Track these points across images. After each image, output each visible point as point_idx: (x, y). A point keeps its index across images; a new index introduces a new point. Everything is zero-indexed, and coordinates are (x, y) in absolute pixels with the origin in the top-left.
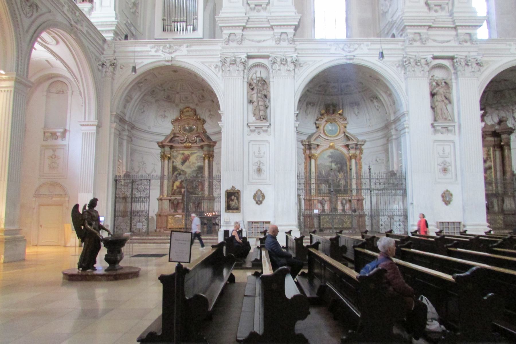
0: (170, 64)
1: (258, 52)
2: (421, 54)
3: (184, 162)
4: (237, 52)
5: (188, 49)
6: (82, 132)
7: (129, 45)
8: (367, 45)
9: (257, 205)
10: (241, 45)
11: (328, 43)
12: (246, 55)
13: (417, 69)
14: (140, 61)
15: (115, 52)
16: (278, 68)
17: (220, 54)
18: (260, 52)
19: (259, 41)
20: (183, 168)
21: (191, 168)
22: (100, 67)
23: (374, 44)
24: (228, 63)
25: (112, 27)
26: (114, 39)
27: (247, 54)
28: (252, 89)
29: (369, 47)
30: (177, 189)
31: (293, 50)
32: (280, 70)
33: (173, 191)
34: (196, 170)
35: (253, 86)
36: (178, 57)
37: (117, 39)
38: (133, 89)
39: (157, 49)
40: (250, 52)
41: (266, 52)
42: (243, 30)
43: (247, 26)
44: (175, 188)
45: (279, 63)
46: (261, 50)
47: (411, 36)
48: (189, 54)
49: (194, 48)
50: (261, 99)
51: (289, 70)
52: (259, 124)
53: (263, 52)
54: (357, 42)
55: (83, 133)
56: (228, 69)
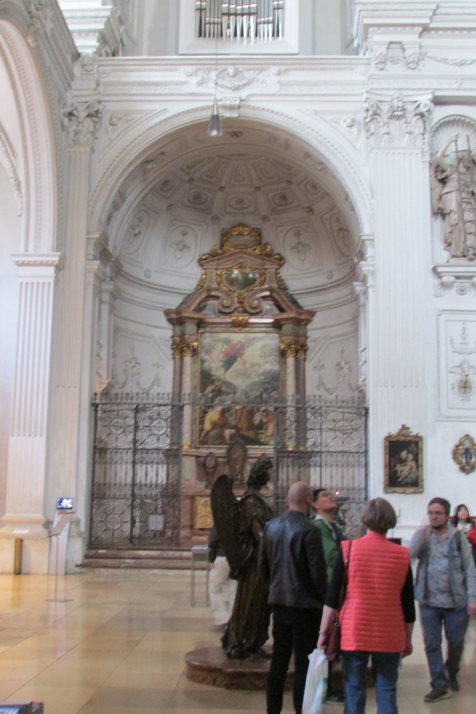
0: (235, 114)
1: (458, 89)
4: (407, 89)
6: (20, 280)
7: (133, 68)
9: (463, 475)
10: (416, 72)
12: (430, 96)
14: (159, 107)
15: (98, 85)
17: (367, 92)
18: (465, 90)
19: (462, 64)
21: (248, 377)
22: (66, 120)
24: (385, 116)
25: (96, 22)
26: (98, 53)
27: (433, 93)
28: (443, 181)
30: (212, 429)
34: (262, 383)
35: (445, 174)
36: (252, 99)
38: (132, 177)
40: (439, 90)
42: (420, 35)
43: (432, 25)
44: (207, 426)
48: (282, 92)
49: (294, 76)
50: (469, 206)
55: (21, 284)
56: (385, 130)
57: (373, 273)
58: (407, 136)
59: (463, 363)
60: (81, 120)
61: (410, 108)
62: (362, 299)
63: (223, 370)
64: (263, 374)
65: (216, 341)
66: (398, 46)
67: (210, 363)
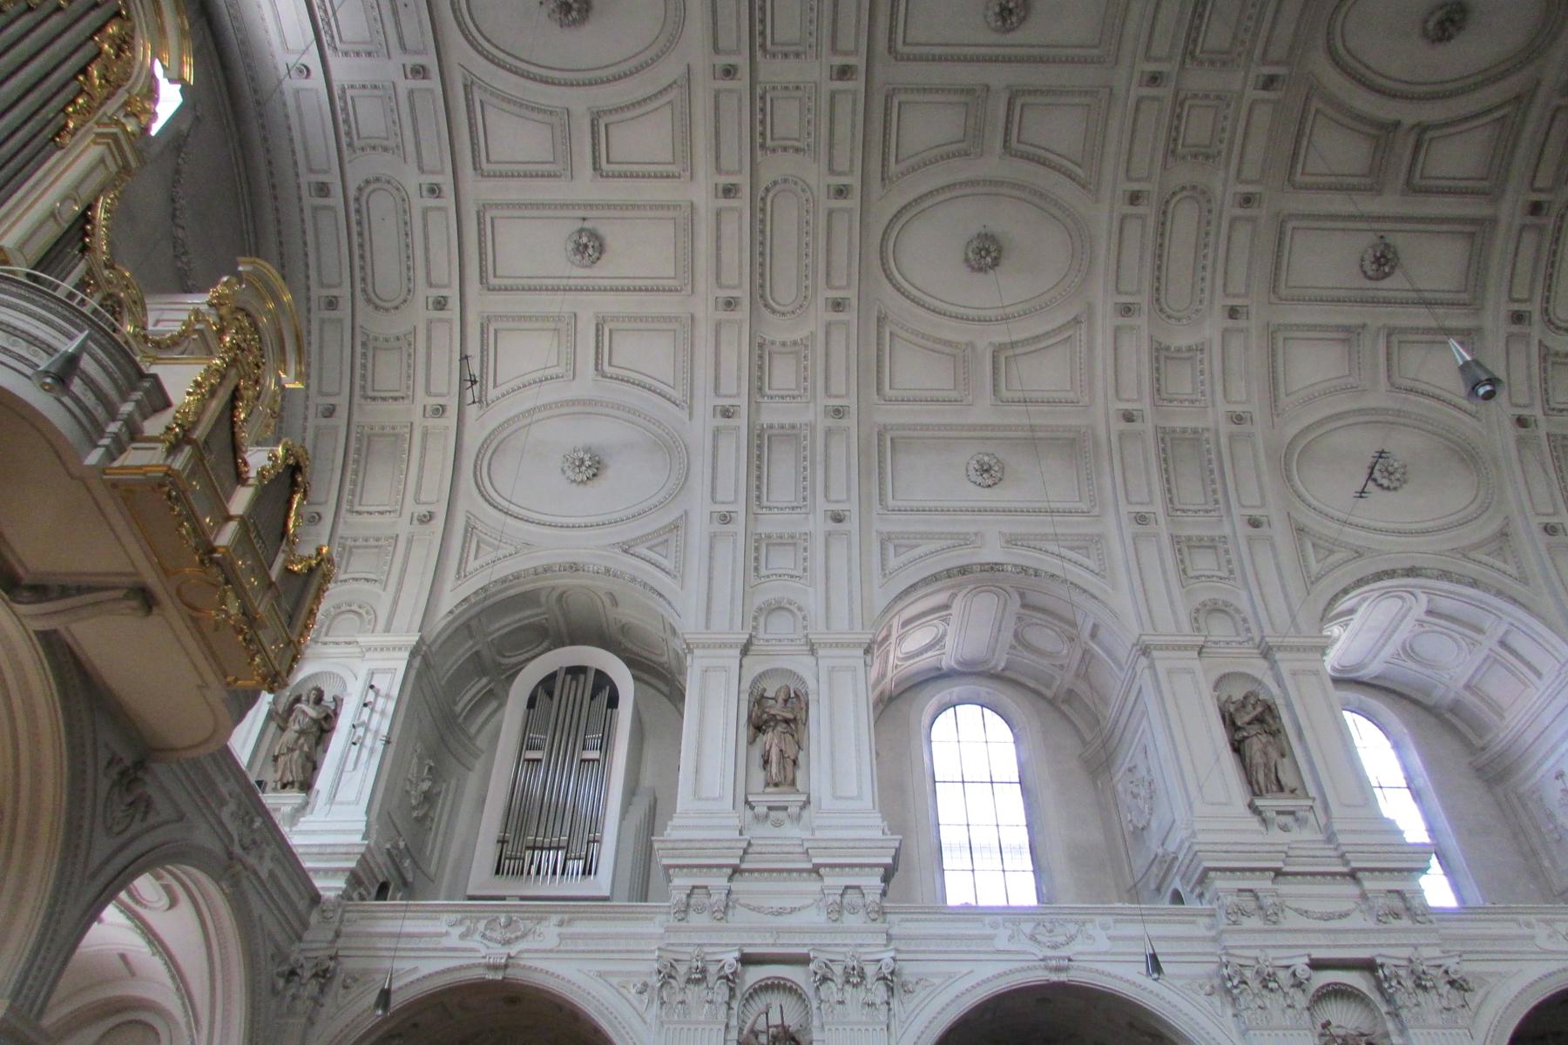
0: (499, 976)
1: (774, 945)
2: (1272, 953)
5: (564, 930)
7: (386, 915)
8: (1104, 927)
10: (723, 924)
11: (987, 919)
12: (737, 954)
13: (1268, 999)
14: (407, 965)
15: (338, 935)
16: (838, 997)
17: (659, 949)
18: (782, 945)
19: (780, 912)
22: (281, 983)
23: (1122, 921)
24: (681, 980)
25: (347, 860)
26: (346, 896)
29: (1111, 932)
31: (882, 939)
32: (841, 1002)
36: (526, 955)
37: (355, 895)
39: (468, 929)
40: (750, 945)
41: (797, 945)
42: (730, 879)
43: (744, 866)
45: (839, 981)
46: (785, 939)
47: (1230, 900)
48: (562, 948)
49: (581, 927)
51: (871, 1005)
54: (1074, 917)
56: (680, 997)
58: (707, 1005)
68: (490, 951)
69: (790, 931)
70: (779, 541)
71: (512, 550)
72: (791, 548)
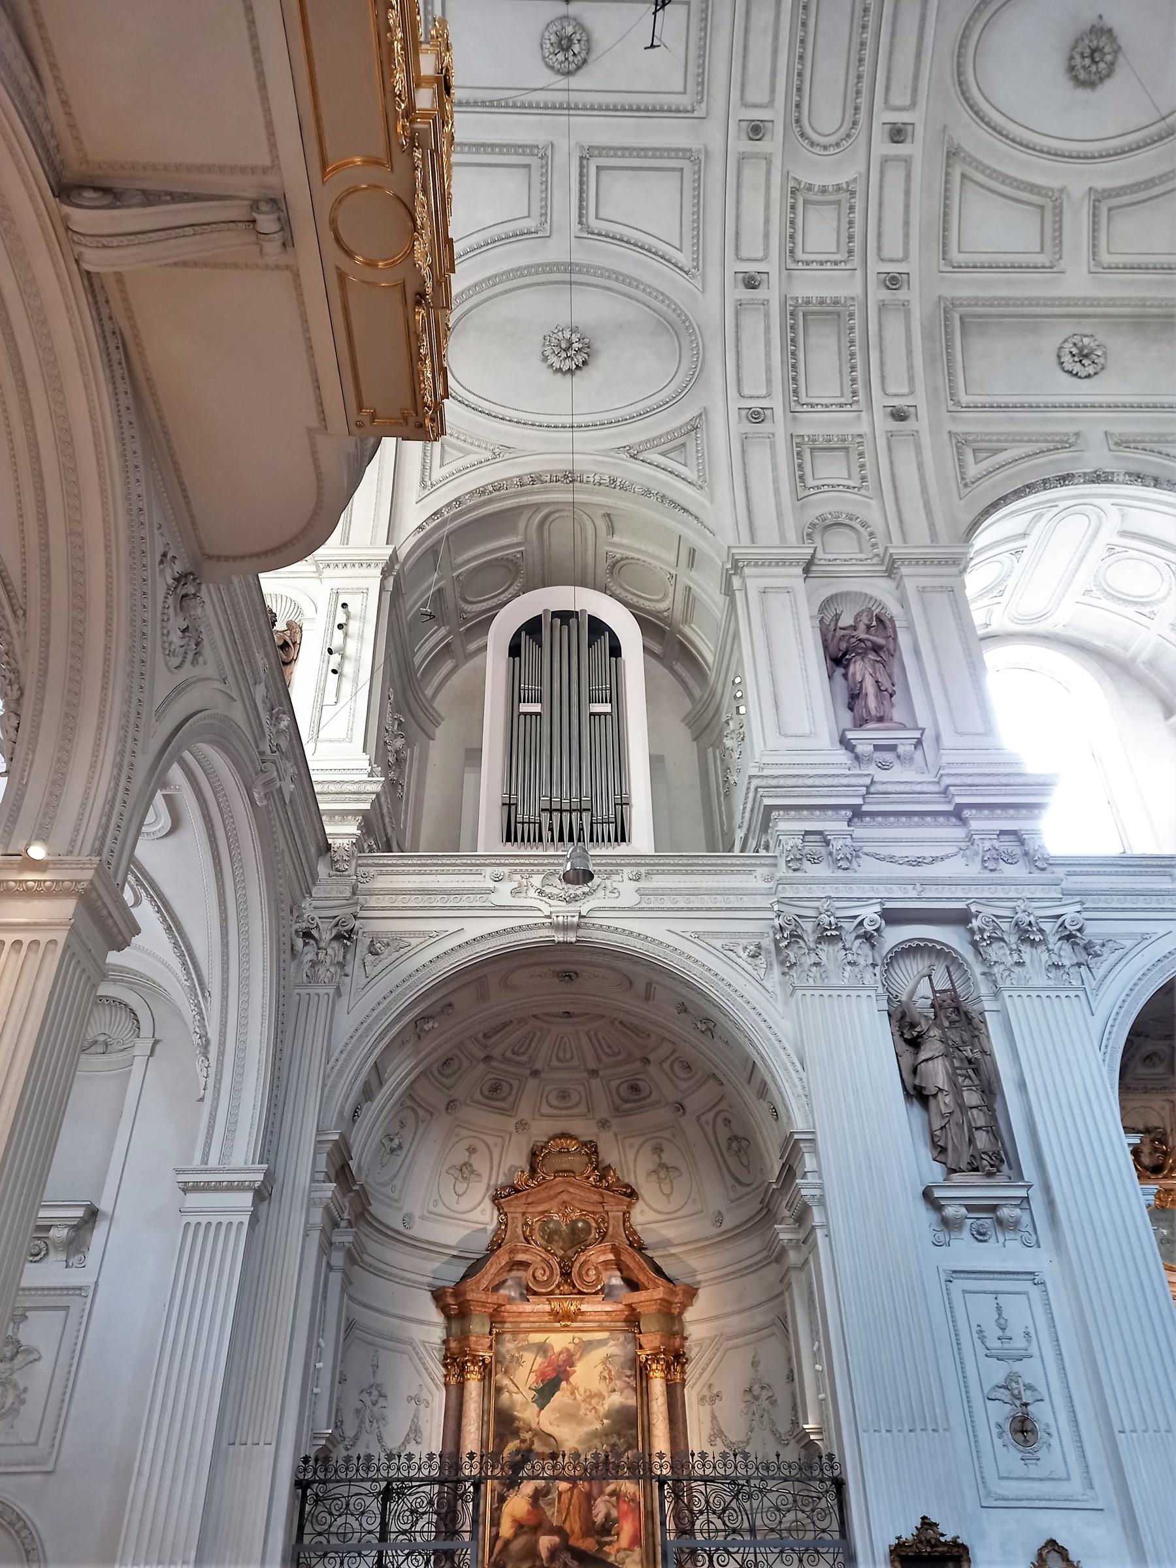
1: (919, 899)
3: (546, 1390)
4: (839, 899)
6: (186, 1219)
10: (850, 874)
12: (878, 908)
15: (354, 893)
19: (918, 862)
20: (547, 1420)
21: (580, 1422)
22: (299, 942)
24: (810, 938)
26: (358, 845)
28: (915, 1043)
33: (499, 1545)
34: (606, 1434)
38: (398, 1042)
43: (865, 808)
44: (506, 1530)
46: (931, 892)
48: (643, 905)
50: (967, 1082)
52: (978, 1189)
53: (938, 899)
56: (813, 958)
57: (822, 1201)
58: (848, 968)
59: (1012, 1377)
60: (322, 945)
61: (849, 926)
62: (793, 1257)
63: (536, 1408)
64: (607, 1416)
65: (522, 1348)
66: (818, 838)
67: (510, 1393)
68: (552, 909)
69: (937, 882)
70: (825, 445)
71: (489, 455)
72: (842, 454)
